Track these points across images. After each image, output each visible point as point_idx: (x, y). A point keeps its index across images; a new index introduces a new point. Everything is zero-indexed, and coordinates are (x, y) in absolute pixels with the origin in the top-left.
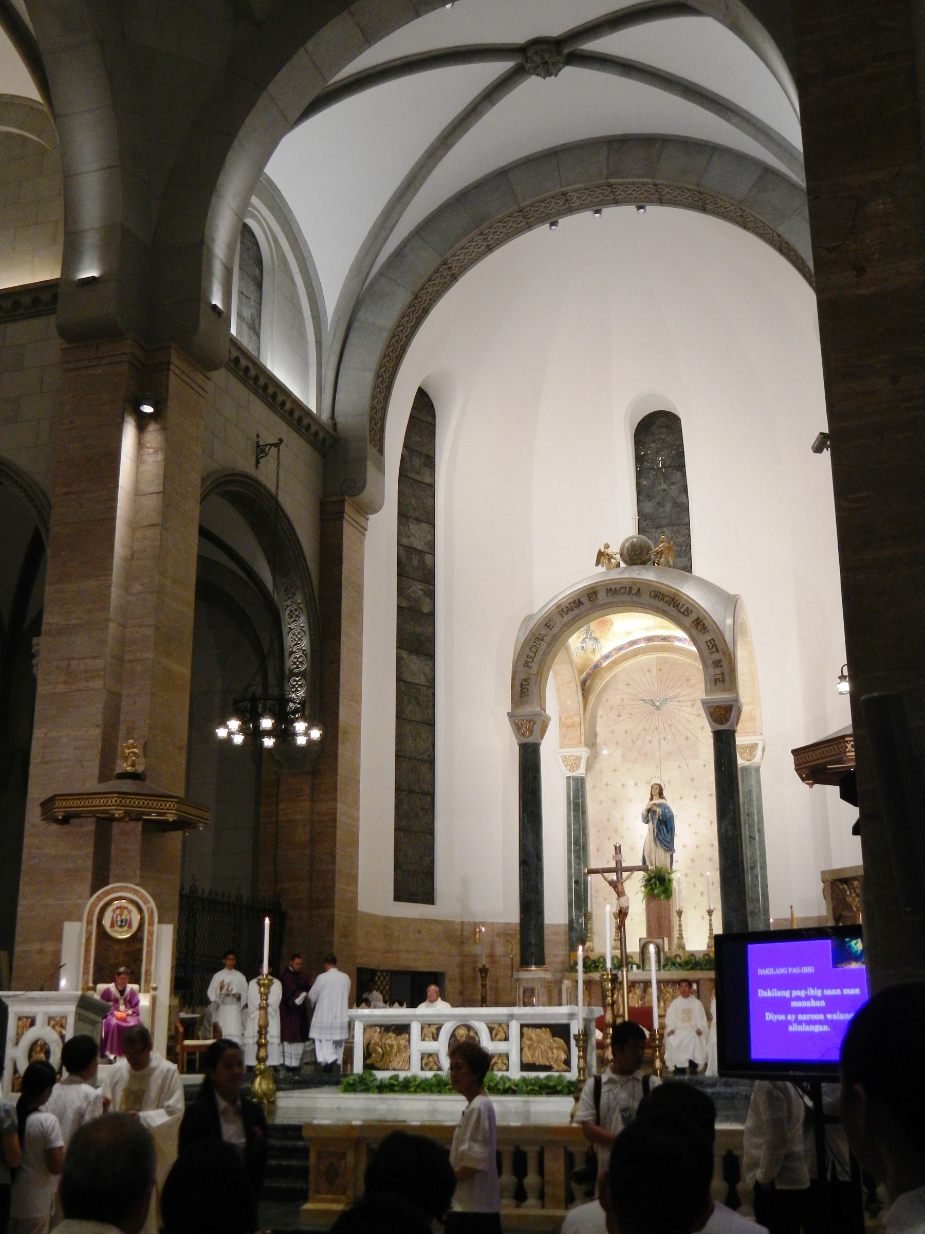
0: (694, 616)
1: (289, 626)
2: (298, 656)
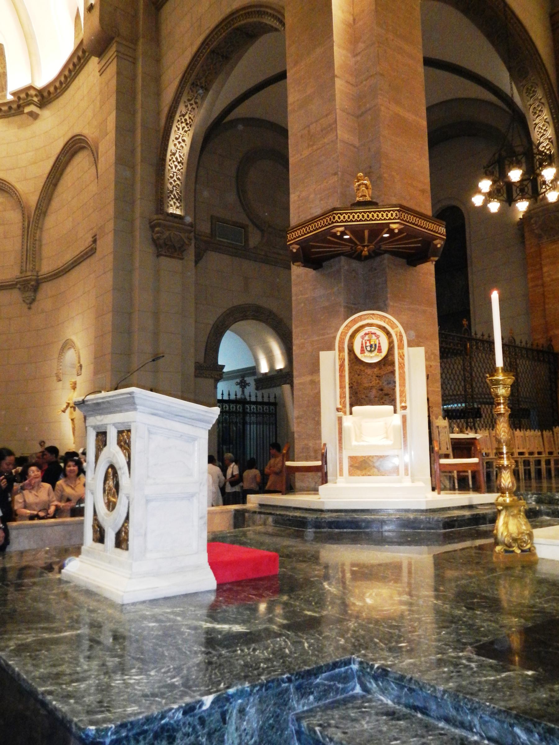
1: (534, 122)
2: (545, 145)
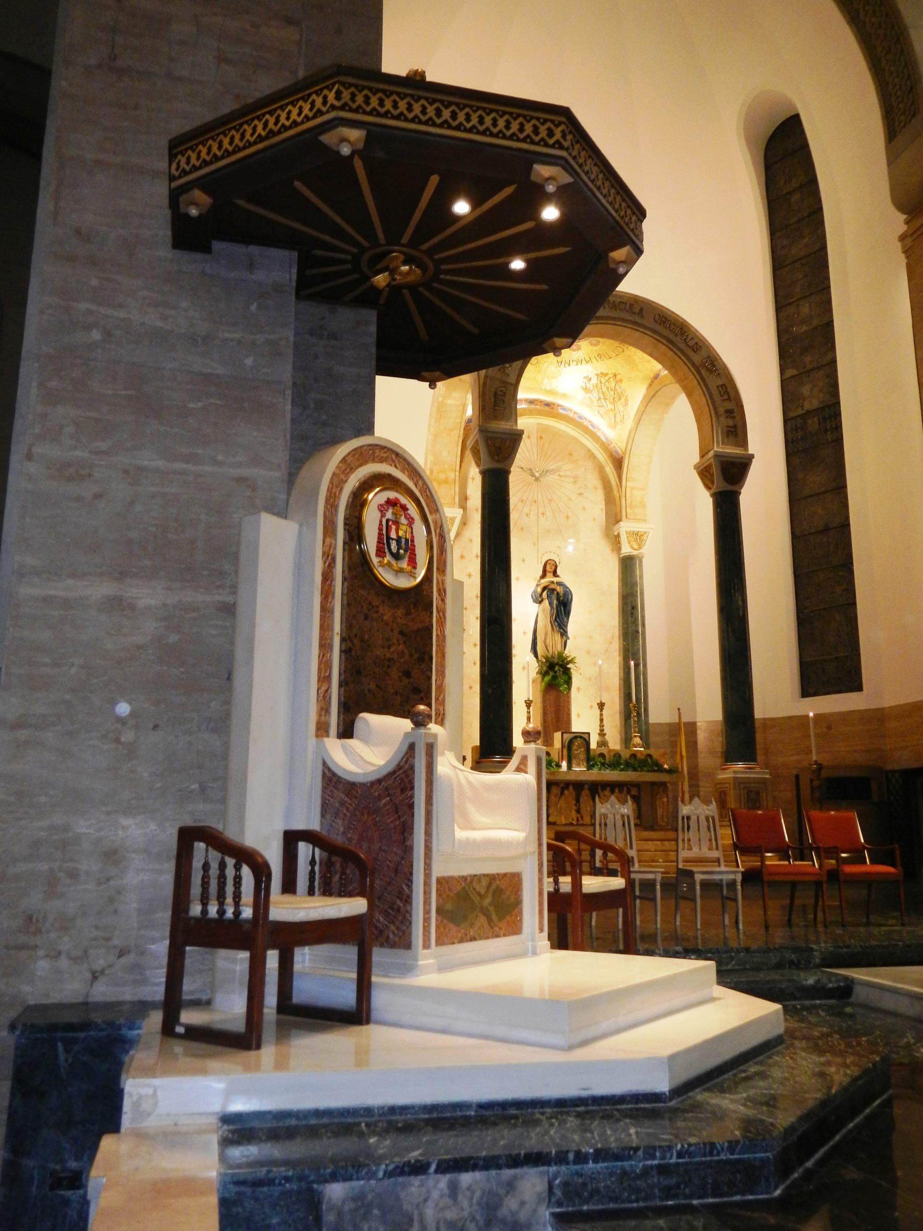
0: (704, 353)
